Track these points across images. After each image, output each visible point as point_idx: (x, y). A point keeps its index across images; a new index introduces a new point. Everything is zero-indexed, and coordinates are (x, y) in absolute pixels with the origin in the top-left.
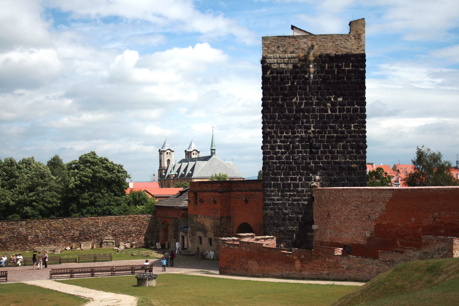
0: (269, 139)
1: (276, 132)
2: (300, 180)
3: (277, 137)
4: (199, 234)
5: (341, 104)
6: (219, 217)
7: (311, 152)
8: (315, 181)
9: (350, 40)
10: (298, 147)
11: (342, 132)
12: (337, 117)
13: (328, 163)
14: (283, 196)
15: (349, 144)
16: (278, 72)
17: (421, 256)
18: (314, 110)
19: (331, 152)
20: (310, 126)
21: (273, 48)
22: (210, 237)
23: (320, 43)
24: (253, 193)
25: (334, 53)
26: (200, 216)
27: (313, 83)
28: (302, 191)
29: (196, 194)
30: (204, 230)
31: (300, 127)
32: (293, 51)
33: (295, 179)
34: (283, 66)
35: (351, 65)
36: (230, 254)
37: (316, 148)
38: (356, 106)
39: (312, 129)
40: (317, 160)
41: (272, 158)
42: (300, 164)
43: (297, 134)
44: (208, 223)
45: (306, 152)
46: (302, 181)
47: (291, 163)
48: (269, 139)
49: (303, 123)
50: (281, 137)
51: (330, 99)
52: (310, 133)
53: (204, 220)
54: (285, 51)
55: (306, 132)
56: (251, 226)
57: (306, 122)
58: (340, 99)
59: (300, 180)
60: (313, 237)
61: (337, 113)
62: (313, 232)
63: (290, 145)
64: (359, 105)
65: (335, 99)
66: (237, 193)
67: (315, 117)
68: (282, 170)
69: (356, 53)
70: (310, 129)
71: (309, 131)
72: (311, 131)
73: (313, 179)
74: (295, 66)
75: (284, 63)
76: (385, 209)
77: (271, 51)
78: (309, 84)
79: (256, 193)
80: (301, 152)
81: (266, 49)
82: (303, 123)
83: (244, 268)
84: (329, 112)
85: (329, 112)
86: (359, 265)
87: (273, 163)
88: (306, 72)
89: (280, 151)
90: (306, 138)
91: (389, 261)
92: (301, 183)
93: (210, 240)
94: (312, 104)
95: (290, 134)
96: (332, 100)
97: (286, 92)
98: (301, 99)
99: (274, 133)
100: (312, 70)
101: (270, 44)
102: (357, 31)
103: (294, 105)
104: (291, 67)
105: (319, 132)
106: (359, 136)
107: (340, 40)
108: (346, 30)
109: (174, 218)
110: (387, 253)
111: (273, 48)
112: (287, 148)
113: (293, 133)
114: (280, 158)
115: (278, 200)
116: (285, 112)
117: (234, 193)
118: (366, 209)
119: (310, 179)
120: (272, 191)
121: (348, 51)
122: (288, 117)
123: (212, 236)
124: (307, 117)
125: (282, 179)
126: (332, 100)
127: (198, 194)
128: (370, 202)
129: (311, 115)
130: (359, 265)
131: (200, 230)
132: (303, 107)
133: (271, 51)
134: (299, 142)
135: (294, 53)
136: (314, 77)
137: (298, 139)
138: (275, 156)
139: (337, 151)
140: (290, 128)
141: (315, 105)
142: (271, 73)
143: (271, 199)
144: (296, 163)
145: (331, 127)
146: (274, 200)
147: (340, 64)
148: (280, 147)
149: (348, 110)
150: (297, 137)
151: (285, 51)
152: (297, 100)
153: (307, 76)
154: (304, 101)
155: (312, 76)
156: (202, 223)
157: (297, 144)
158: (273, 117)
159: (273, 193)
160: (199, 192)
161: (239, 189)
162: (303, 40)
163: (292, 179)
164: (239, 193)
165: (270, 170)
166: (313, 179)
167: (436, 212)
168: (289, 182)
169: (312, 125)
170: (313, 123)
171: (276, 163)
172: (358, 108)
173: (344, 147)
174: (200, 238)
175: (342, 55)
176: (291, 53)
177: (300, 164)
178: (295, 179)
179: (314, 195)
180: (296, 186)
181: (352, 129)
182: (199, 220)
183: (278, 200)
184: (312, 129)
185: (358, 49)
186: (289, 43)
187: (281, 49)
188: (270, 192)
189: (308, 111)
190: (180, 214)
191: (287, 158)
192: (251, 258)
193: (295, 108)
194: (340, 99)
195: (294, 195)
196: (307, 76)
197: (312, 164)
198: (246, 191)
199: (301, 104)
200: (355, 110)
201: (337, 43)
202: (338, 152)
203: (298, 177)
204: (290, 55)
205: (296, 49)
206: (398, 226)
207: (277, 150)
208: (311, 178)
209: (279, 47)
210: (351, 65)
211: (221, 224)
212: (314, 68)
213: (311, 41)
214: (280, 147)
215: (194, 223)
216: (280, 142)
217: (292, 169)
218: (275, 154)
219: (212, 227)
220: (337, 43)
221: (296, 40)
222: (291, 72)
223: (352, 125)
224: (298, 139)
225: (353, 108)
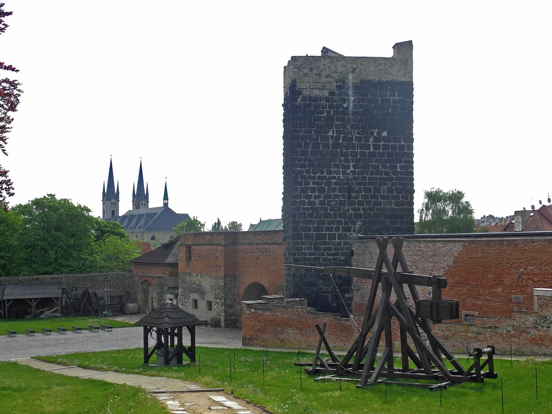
0: (299, 180)
1: (308, 172)
2: (337, 229)
3: (310, 177)
4: (194, 296)
5: (385, 139)
6: (223, 275)
7: (349, 197)
8: (354, 231)
10: (334, 190)
11: (387, 174)
12: (381, 155)
13: (370, 209)
14: (316, 249)
15: (394, 187)
16: (311, 99)
17: (537, 321)
18: (354, 147)
19: (373, 197)
21: (305, 71)
22: (210, 300)
23: (361, 67)
24: (268, 246)
25: (377, 79)
26: (195, 275)
27: (354, 114)
28: (339, 244)
29: (190, 247)
30: (201, 292)
31: (337, 166)
32: (329, 75)
33: (331, 229)
34: (316, 92)
35: (396, 94)
36: (259, 321)
37: (356, 192)
38: (403, 143)
39: (352, 169)
40: (357, 206)
44: (207, 283)
45: (343, 196)
48: (299, 180)
50: (314, 178)
51: (372, 133)
53: (200, 279)
54: (319, 74)
55: (344, 173)
56: (265, 285)
58: (385, 134)
59: (337, 229)
60: (351, 299)
61: (381, 150)
62: (352, 293)
64: (405, 142)
65: (379, 133)
66: (245, 247)
67: (355, 155)
68: (316, 218)
71: (347, 172)
73: (352, 230)
74: (332, 93)
75: (319, 89)
76: (451, 264)
77: (302, 74)
79: (272, 246)
80: (337, 196)
81: (297, 70)
82: (340, 161)
83: (278, 339)
84: (372, 150)
85: (372, 150)
86: (447, 333)
87: (304, 209)
88: (344, 101)
89: (313, 194)
90: (344, 180)
91: (490, 327)
93: (210, 304)
94: (351, 139)
95: (325, 174)
96: (375, 135)
97: (320, 123)
98: (339, 132)
100: (352, 98)
101: (301, 65)
103: (330, 140)
104: (326, 94)
105: (359, 173)
106: (406, 178)
107: (385, 64)
108: (389, 53)
109: (159, 277)
110: (488, 317)
111: (305, 71)
112: (321, 190)
113: (330, 172)
115: (311, 254)
117: (240, 246)
118: (425, 265)
119: (349, 229)
120: (303, 244)
123: (212, 299)
124: (346, 155)
125: (315, 229)
126: (375, 135)
127: (192, 247)
128: (431, 257)
129: (351, 152)
130: (447, 333)
131: (195, 291)
132: (340, 141)
133: (302, 74)
134: (336, 183)
135: (330, 77)
136: (354, 108)
137: (335, 181)
138: (307, 201)
139: (381, 196)
141: (355, 141)
142: (304, 99)
144: (332, 209)
145: (373, 167)
146: (305, 254)
147: (384, 93)
148: (313, 190)
149: (394, 147)
150: (334, 178)
151: (319, 74)
152: (333, 133)
153: (345, 105)
154: (342, 136)
155: (351, 104)
156: (198, 283)
159: (304, 247)
160: (194, 245)
161: (247, 241)
162: (341, 63)
163: (328, 229)
164: (248, 247)
166: (352, 230)
167: (522, 268)
168: (324, 232)
169: (351, 164)
170: (353, 162)
171: (307, 209)
172: (405, 146)
173: (390, 190)
174: (196, 302)
175: (387, 81)
176: (326, 77)
178: (331, 229)
179: (354, 249)
180: (333, 237)
181: (398, 169)
182: (194, 279)
183: (311, 254)
184: (352, 169)
185: (405, 75)
186: (324, 65)
187: (315, 72)
189: (347, 148)
190: (167, 273)
191: (322, 203)
192: (290, 326)
193: (331, 143)
194: (385, 134)
195: (330, 249)
196: (345, 105)
198: (257, 244)
199: (338, 138)
200: (402, 147)
201: (381, 67)
202: (382, 197)
203: (334, 227)
204: (324, 80)
205: (333, 72)
206: (470, 284)
207: (310, 194)
208: (350, 228)
209: (311, 69)
210: (396, 94)
211: (225, 284)
212: (354, 96)
213: (351, 63)
214: (313, 190)
215: (187, 283)
216: (313, 184)
217: (327, 216)
219: (212, 287)
220: (381, 67)
221: (333, 62)
222: (327, 99)
223: (398, 165)
224: (335, 181)
225: (399, 145)
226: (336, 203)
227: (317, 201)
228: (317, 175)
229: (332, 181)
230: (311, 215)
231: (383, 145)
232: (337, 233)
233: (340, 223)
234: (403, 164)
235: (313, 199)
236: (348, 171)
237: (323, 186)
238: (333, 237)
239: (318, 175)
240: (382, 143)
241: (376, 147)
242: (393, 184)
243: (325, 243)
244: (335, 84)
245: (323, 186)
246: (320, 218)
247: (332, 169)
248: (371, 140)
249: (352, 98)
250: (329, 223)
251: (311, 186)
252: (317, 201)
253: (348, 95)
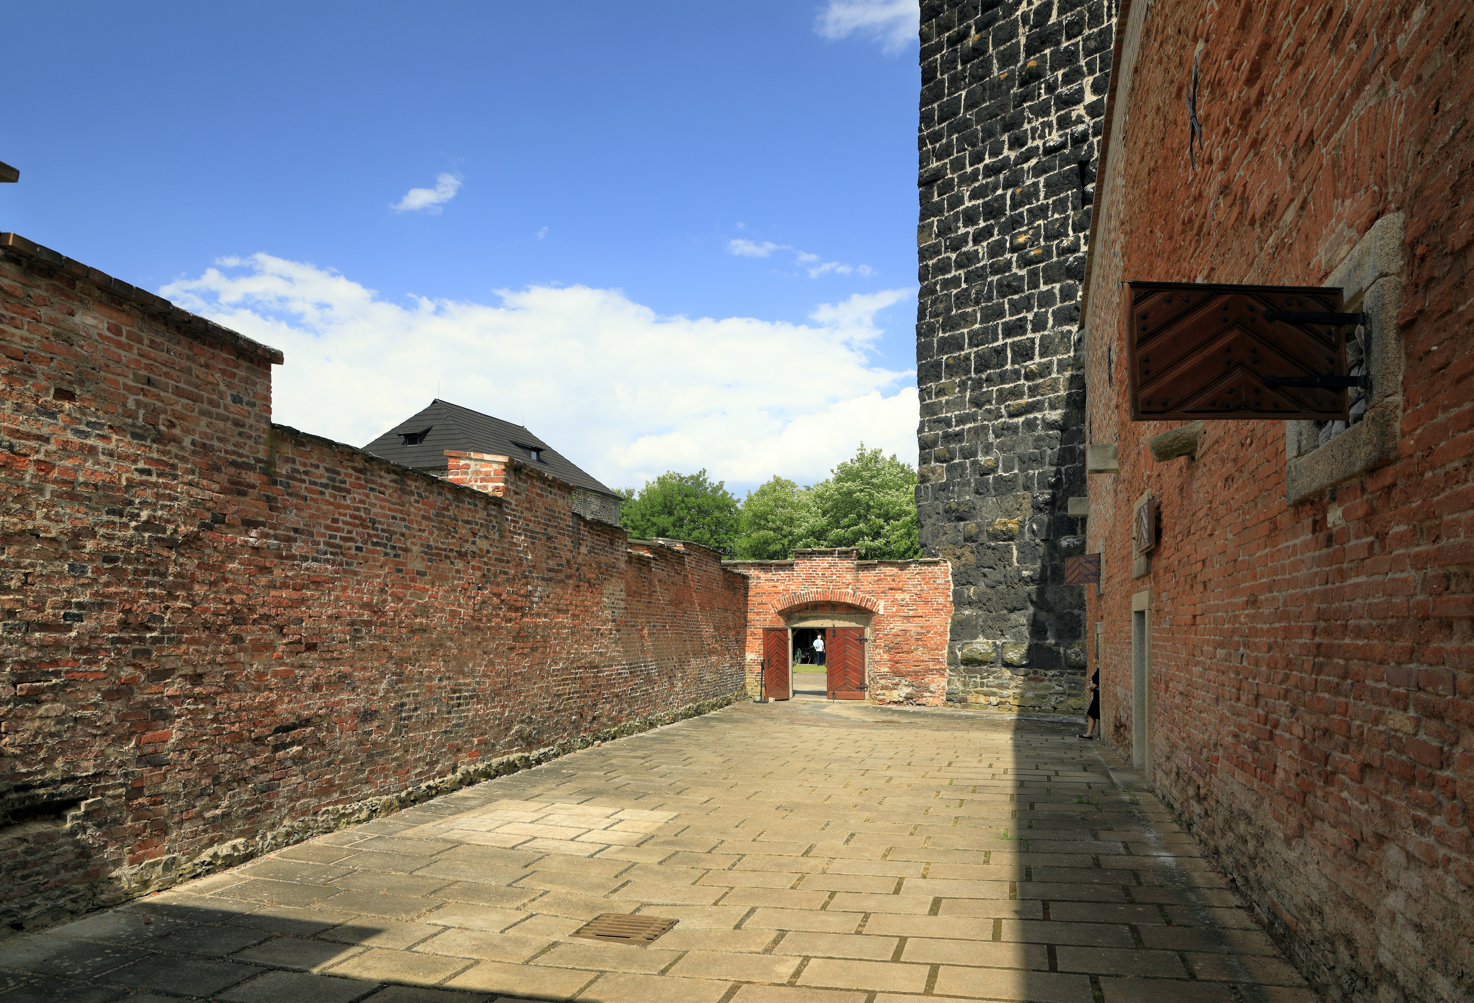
0: (936, 198)
1: (957, 166)
2: (1039, 324)
10: (1032, 193)
20: (1081, 91)
33: (1018, 328)
39: (1090, 98)
41: (943, 267)
42: (1037, 260)
43: (1030, 144)
46: (1044, 328)
47: (1008, 264)
48: (936, 198)
49: (1051, 88)
52: (1080, 120)
55: (1064, 122)
57: (1068, 79)
59: (1039, 324)
63: (1003, 196)
71: (1074, 115)
72: (1083, 112)
89: (971, 230)
92: (1042, 338)
95: (1006, 152)
99: (953, 171)
112: (993, 211)
113: (1017, 142)
114: (972, 258)
116: (989, 71)
122: (998, 88)
125: (975, 340)
132: (1053, 19)
134: (1038, 170)
137: (1034, 161)
138: (954, 256)
140: (1007, 127)
143: (939, 421)
144: (1025, 262)
146: (948, 422)
148: (970, 218)
157: (1028, 182)
158: (949, 112)
159: (944, 399)
163: (1010, 330)
165: (937, 315)
169: (1089, 80)
170: (1091, 72)
177: (1037, 260)
183: (961, 420)
188: (937, 396)
191: (996, 250)
195: (1016, 393)
203: (1030, 316)
207: (962, 231)
214: (970, 218)
216: (972, 197)
217: (1008, 288)
218: (954, 250)
224: (1034, 161)
227: (982, 248)
228: (981, 166)
229: (1025, 166)
230: (962, 299)
232: (1038, 336)
233: (1046, 299)
235: (970, 247)
236: (1079, 110)
237: (1000, 192)
238: (1024, 353)
239: (987, 161)
243: (1003, 378)
245: (1000, 192)
246: (990, 298)
247: (1026, 126)
250: (1016, 308)
251: (968, 204)
252: (982, 248)
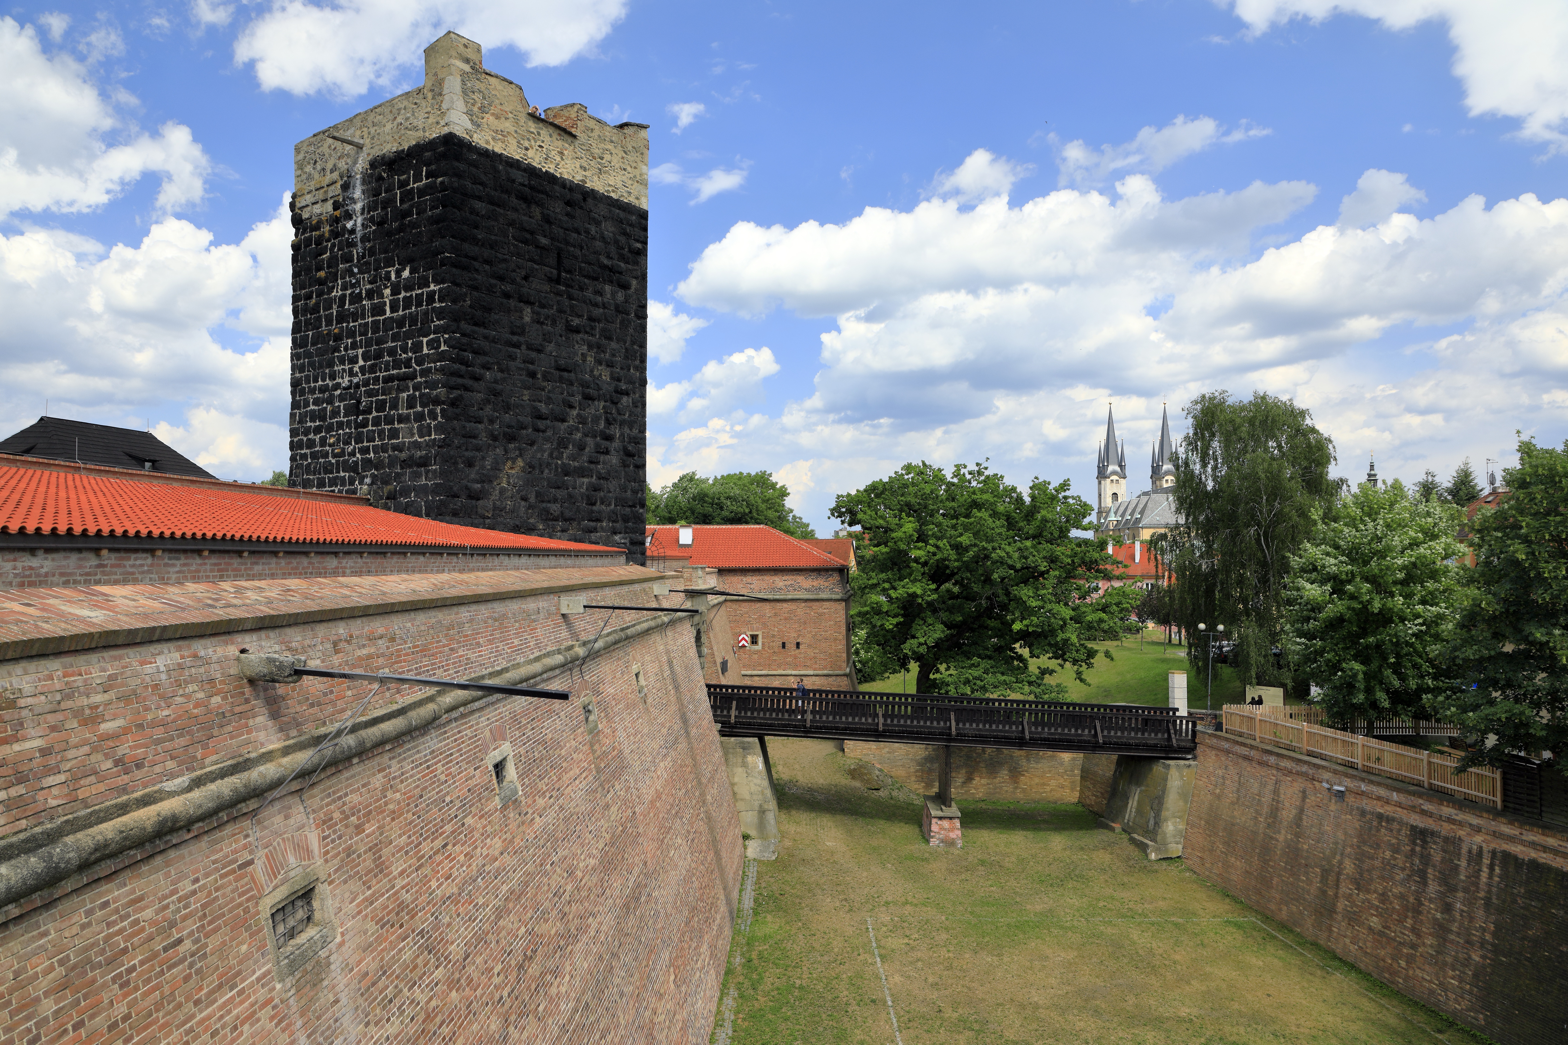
9: (424, 103)
20: (357, 356)
23: (372, 130)
27: (365, 239)
51: (388, 278)
65: (398, 273)
69: (434, 135)
70: (357, 362)
78: (353, 244)
102: (436, 74)
105: (372, 369)
121: (420, 134)
129: (360, 325)
137: (339, 392)
154: (348, 292)
181: (425, 351)
184: (361, 362)
196: (349, 225)
197: (358, 455)
201: (399, 120)
207: (309, 424)
223: (425, 340)
224: (339, 392)
226: (338, 440)
231: (405, 298)
234: (432, 336)
240: (403, 294)
241: (394, 309)
242: (416, 388)
244: (338, 185)
248: (387, 292)
249: (358, 206)
253: (354, 201)
